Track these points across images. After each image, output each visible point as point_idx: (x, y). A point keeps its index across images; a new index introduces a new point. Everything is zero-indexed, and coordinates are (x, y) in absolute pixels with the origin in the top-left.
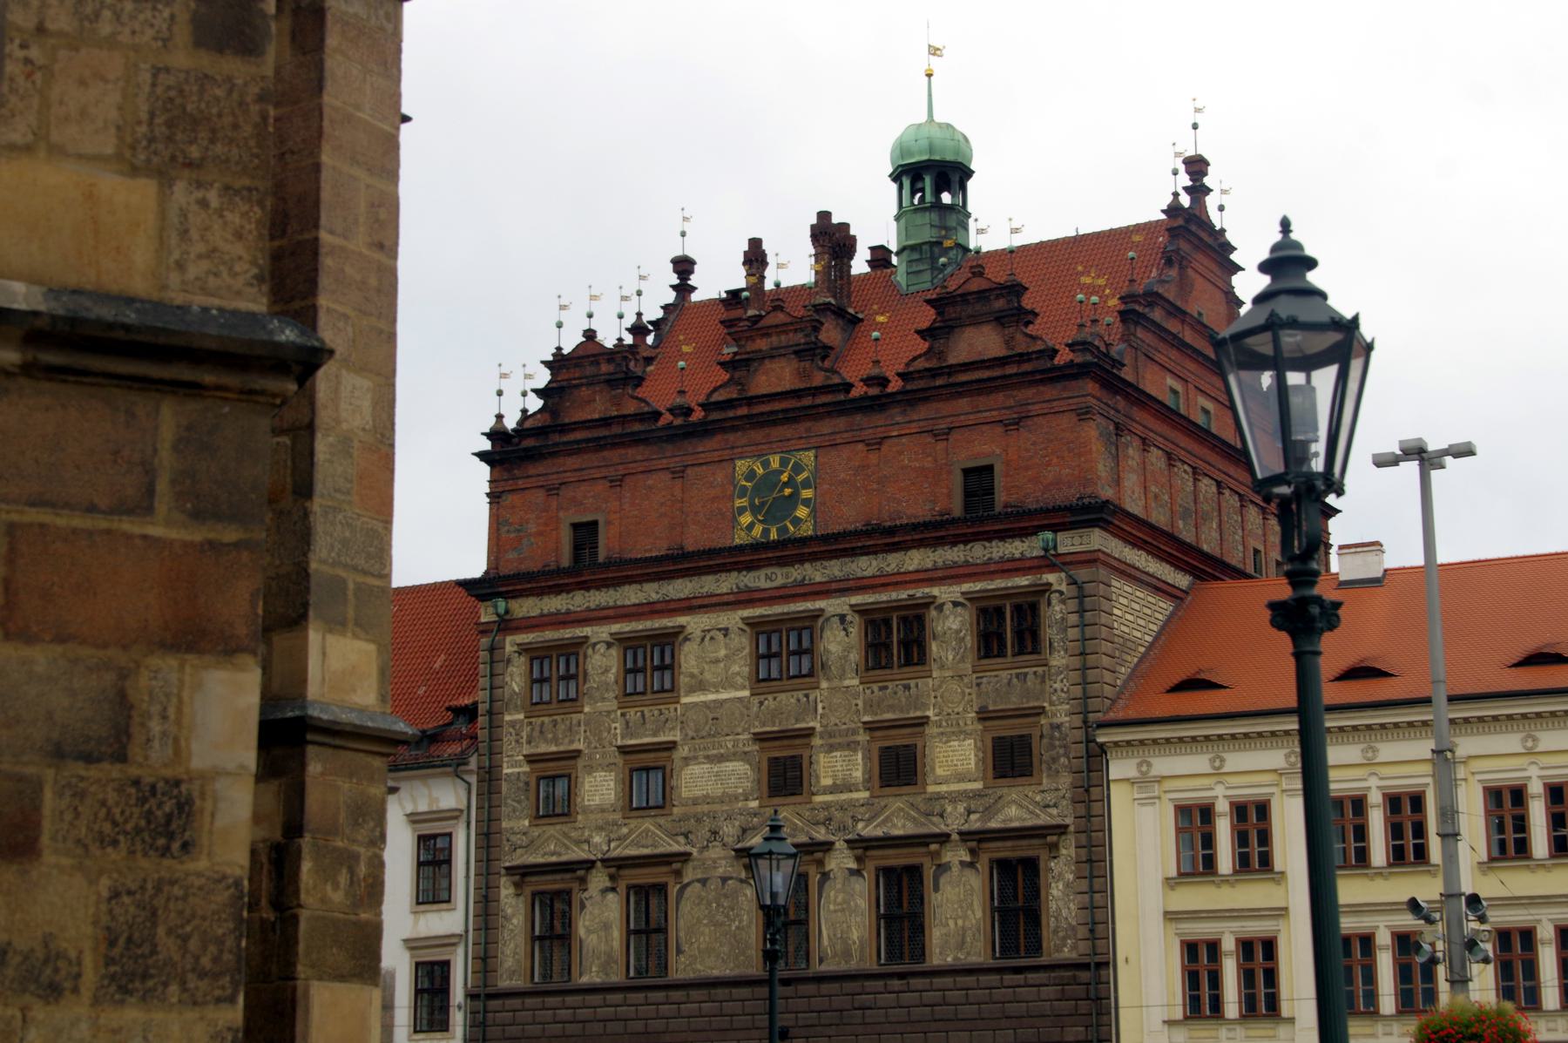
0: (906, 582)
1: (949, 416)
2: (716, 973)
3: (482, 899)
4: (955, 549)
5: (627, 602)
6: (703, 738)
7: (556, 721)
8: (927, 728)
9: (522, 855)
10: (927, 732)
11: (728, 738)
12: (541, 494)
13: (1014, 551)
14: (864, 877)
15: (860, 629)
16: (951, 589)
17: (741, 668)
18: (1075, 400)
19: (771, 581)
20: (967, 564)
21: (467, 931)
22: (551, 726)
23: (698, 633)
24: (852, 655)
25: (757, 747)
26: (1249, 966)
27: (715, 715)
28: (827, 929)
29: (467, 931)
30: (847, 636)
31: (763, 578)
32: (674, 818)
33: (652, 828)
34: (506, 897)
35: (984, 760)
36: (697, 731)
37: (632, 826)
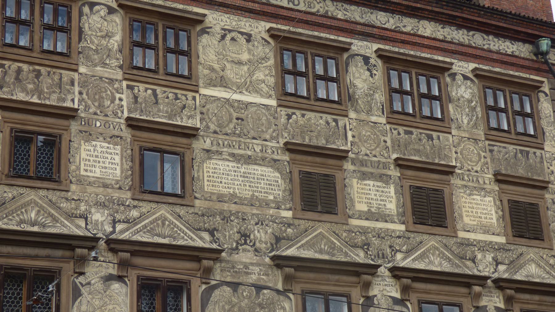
4: (461, 32)
6: (227, 134)
7: (39, 71)
10: (452, 182)
11: (254, 141)
13: (507, 49)
15: (384, 73)
16: (460, 64)
19: (294, 5)
20: (470, 46)
22: (31, 75)
23: (217, 29)
25: (288, 160)
30: (371, 75)
32: (196, 211)
33: (170, 217)
35: (503, 217)
36: (220, 126)
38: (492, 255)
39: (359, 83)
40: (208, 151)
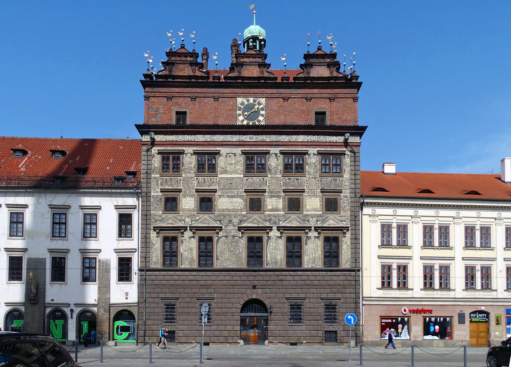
0: (298, 145)
1: (312, 94)
2: (230, 267)
3: (144, 237)
5: (199, 140)
8: (304, 194)
9: (159, 223)
11: (235, 190)
12: (165, 99)
14: (282, 239)
16: (313, 149)
17: (241, 167)
18: (353, 95)
21: (138, 248)
23: (225, 154)
24: (279, 167)
26: (404, 273)
27: (231, 182)
28: (270, 255)
29: (138, 248)
30: (278, 160)
31: (248, 138)
34: (153, 237)
36: (224, 187)
37: (201, 217)
38: (316, 219)
39: (273, 164)
40: (220, 196)
